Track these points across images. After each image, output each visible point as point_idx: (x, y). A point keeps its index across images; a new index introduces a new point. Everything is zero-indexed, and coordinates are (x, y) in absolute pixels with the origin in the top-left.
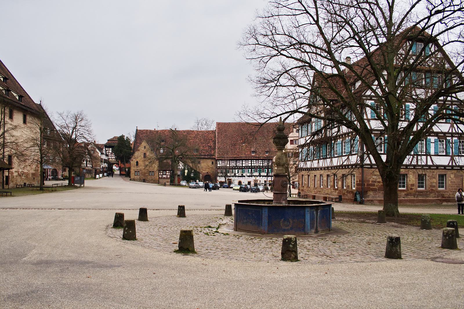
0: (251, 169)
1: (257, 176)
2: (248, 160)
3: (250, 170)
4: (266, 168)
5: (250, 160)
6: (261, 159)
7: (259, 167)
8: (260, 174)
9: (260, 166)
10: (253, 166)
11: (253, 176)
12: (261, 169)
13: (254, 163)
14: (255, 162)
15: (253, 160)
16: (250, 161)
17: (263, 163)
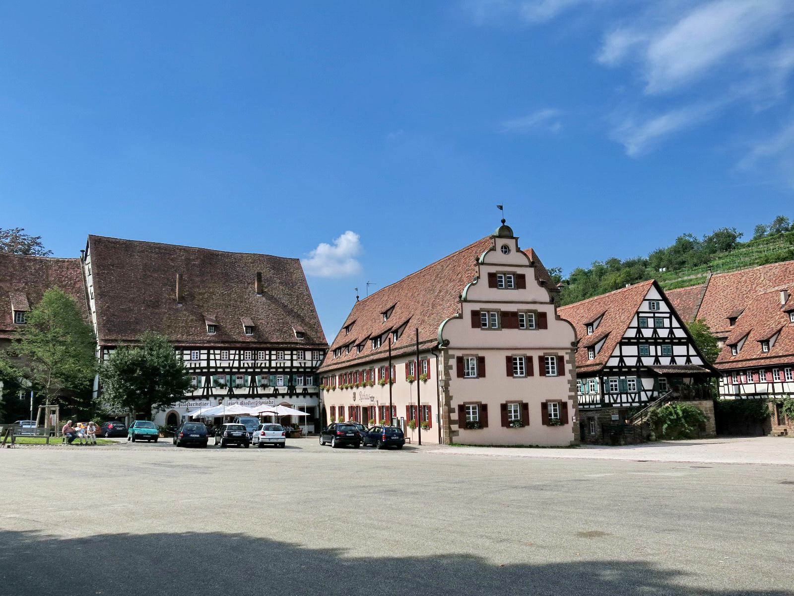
0: (208, 375)
1: (223, 397)
2: (200, 348)
3: (203, 379)
4: (247, 373)
5: (204, 348)
6: (235, 349)
7: (230, 372)
8: (231, 390)
9: (232, 368)
10: (213, 368)
11: (212, 395)
12: (234, 377)
13: (215, 360)
14: (218, 357)
15: (215, 348)
16: (206, 351)
17: (240, 360)
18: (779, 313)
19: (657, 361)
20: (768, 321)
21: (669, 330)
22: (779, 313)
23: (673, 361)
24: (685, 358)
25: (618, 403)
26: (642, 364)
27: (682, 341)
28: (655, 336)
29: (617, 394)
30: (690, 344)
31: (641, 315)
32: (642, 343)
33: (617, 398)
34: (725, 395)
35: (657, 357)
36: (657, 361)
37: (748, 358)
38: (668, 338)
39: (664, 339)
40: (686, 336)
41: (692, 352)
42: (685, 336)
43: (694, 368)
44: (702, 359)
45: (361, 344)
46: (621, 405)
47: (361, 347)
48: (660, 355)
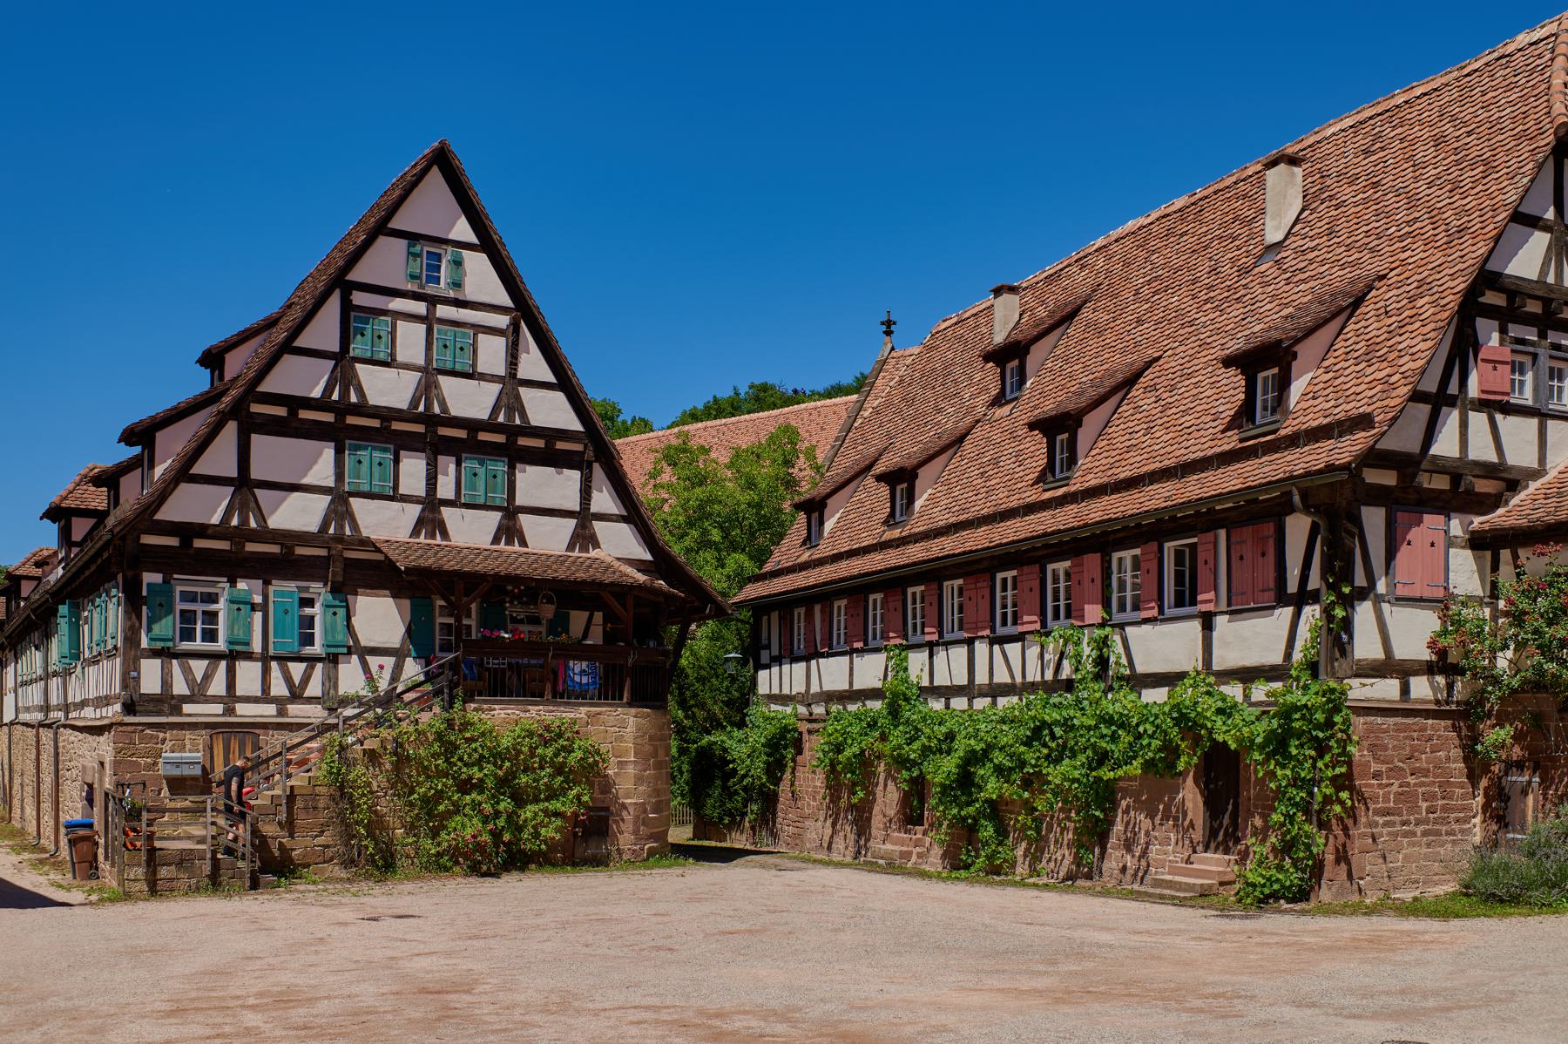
18: (978, 377)
19: (430, 519)
21: (496, 388)
23: (509, 531)
24: (571, 523)
25: (215, 699)
26: (355, 526)
27: (560, 445)
28: (428, 406)
29: (214, 657)
30: (596, 466)
31: (359, 298)
32: (364, 434)
33: (208, 677)
34: (773, 698)
35: (431, 505)
36: (430, 519)
38: (490, 426)
39: (472, 425)
41: (604, 500)
42: (576, 426)
44: (647, 536)
46: (230, 711)
48: (451, 495)
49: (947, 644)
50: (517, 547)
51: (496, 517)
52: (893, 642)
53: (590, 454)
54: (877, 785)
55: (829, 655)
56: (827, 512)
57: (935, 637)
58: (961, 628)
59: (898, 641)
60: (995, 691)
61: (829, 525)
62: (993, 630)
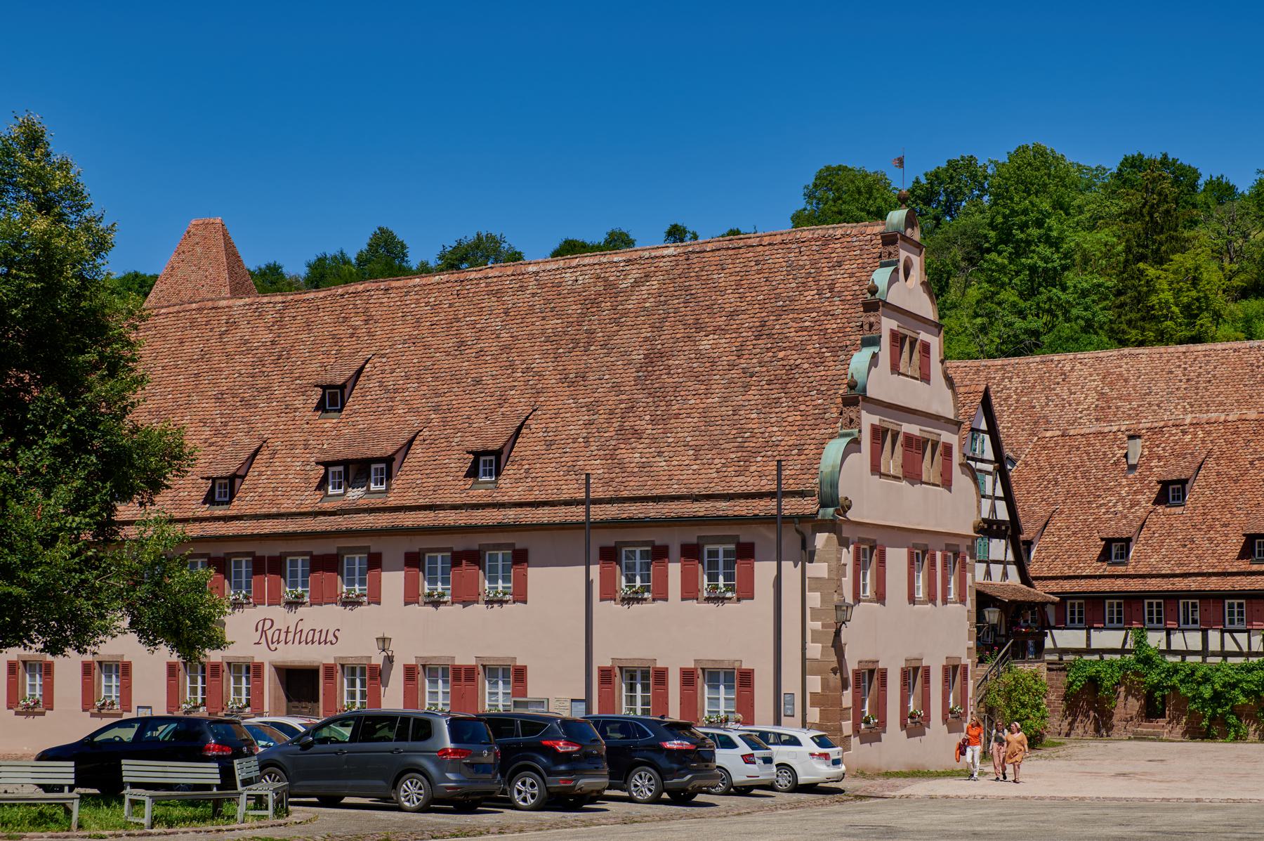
20: (1099, 496)
22: (1124, 482)
23: (988, 574)
37: (1067, 572)
40: (1008, 519)
41: (1010, 557)
43: (1015, 589)
45: (238, 473)
47: (238, 481)
49: (1183, 631)
50: (989, 581)
51: (985, 565)
52: (1134, 626)
53: (1009, 532)
54: (1118, 697)
55: (1064, 629)
56: (1032, 546)
57: (1176, 626)
58: (1195, 622)
59: (1140, 626)
60: (1225, 655)
61: (1033, 554)
62: (1224, 627)
